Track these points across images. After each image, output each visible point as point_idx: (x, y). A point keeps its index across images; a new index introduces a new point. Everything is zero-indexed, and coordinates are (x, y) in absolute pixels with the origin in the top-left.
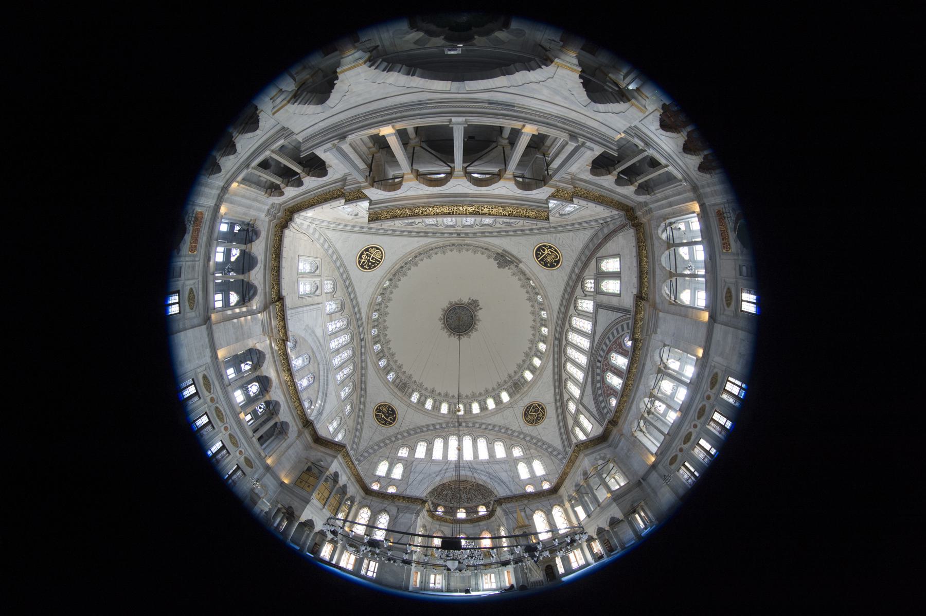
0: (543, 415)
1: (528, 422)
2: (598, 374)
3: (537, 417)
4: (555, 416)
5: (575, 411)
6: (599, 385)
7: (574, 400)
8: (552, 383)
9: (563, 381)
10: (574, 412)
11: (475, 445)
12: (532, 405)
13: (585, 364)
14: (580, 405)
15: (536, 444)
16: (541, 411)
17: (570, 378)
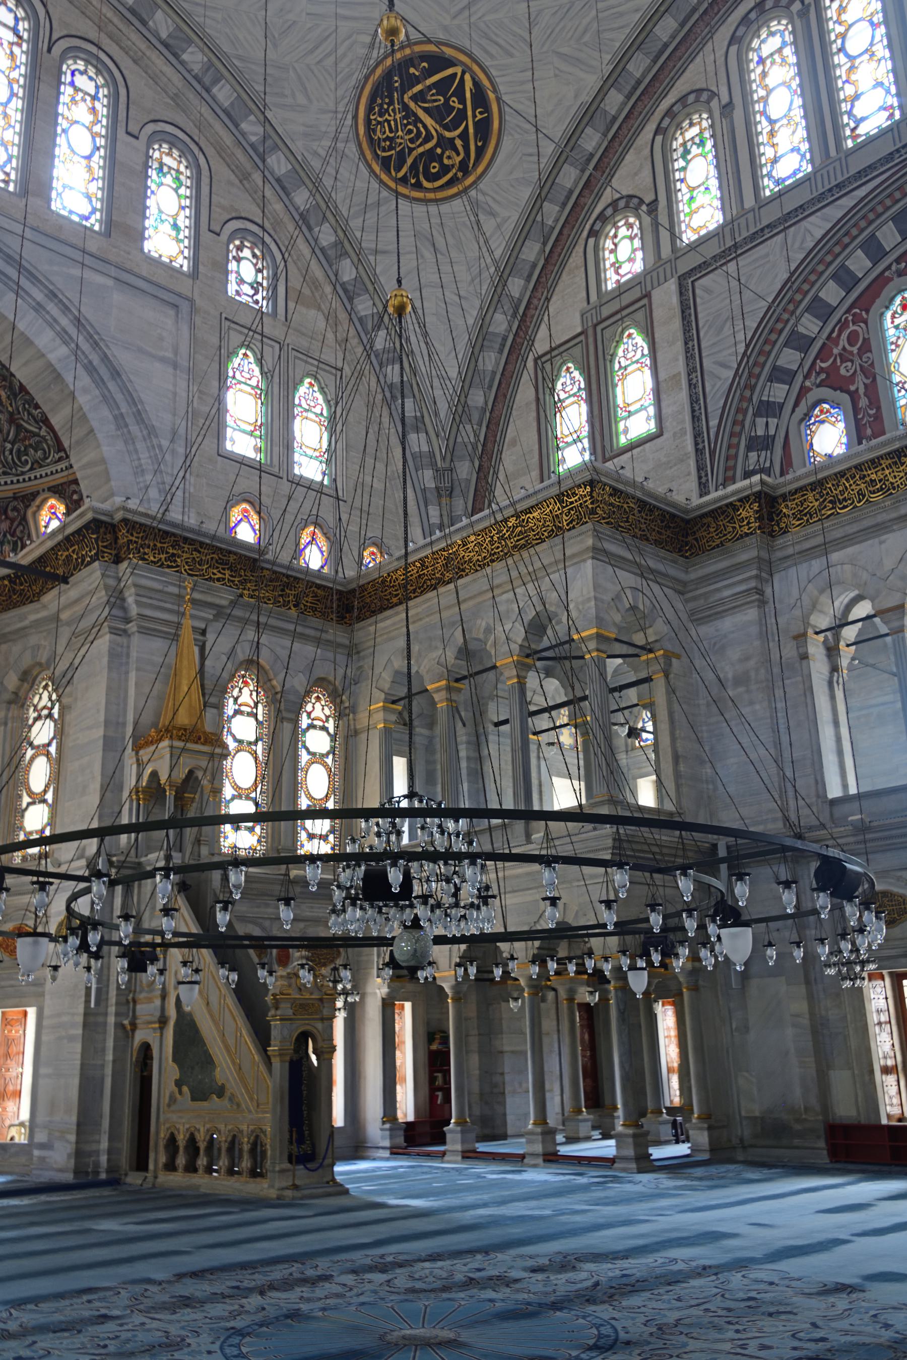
0: (464, 168)
1: (371, 141)
2: (874, 250)
3: (430, 155)
4: (512, 216)
5: (622, 289)
6: (831, 293)
7: (656, 225)
8: (618, 39)
9: (681, 87)
10: (610, 285)
11: (44, 90)
12: (450, 63)
13: (862, 130)
14: (672, 286)
15: (348, 294)
16: (464, 136)
17: (727, 109)
